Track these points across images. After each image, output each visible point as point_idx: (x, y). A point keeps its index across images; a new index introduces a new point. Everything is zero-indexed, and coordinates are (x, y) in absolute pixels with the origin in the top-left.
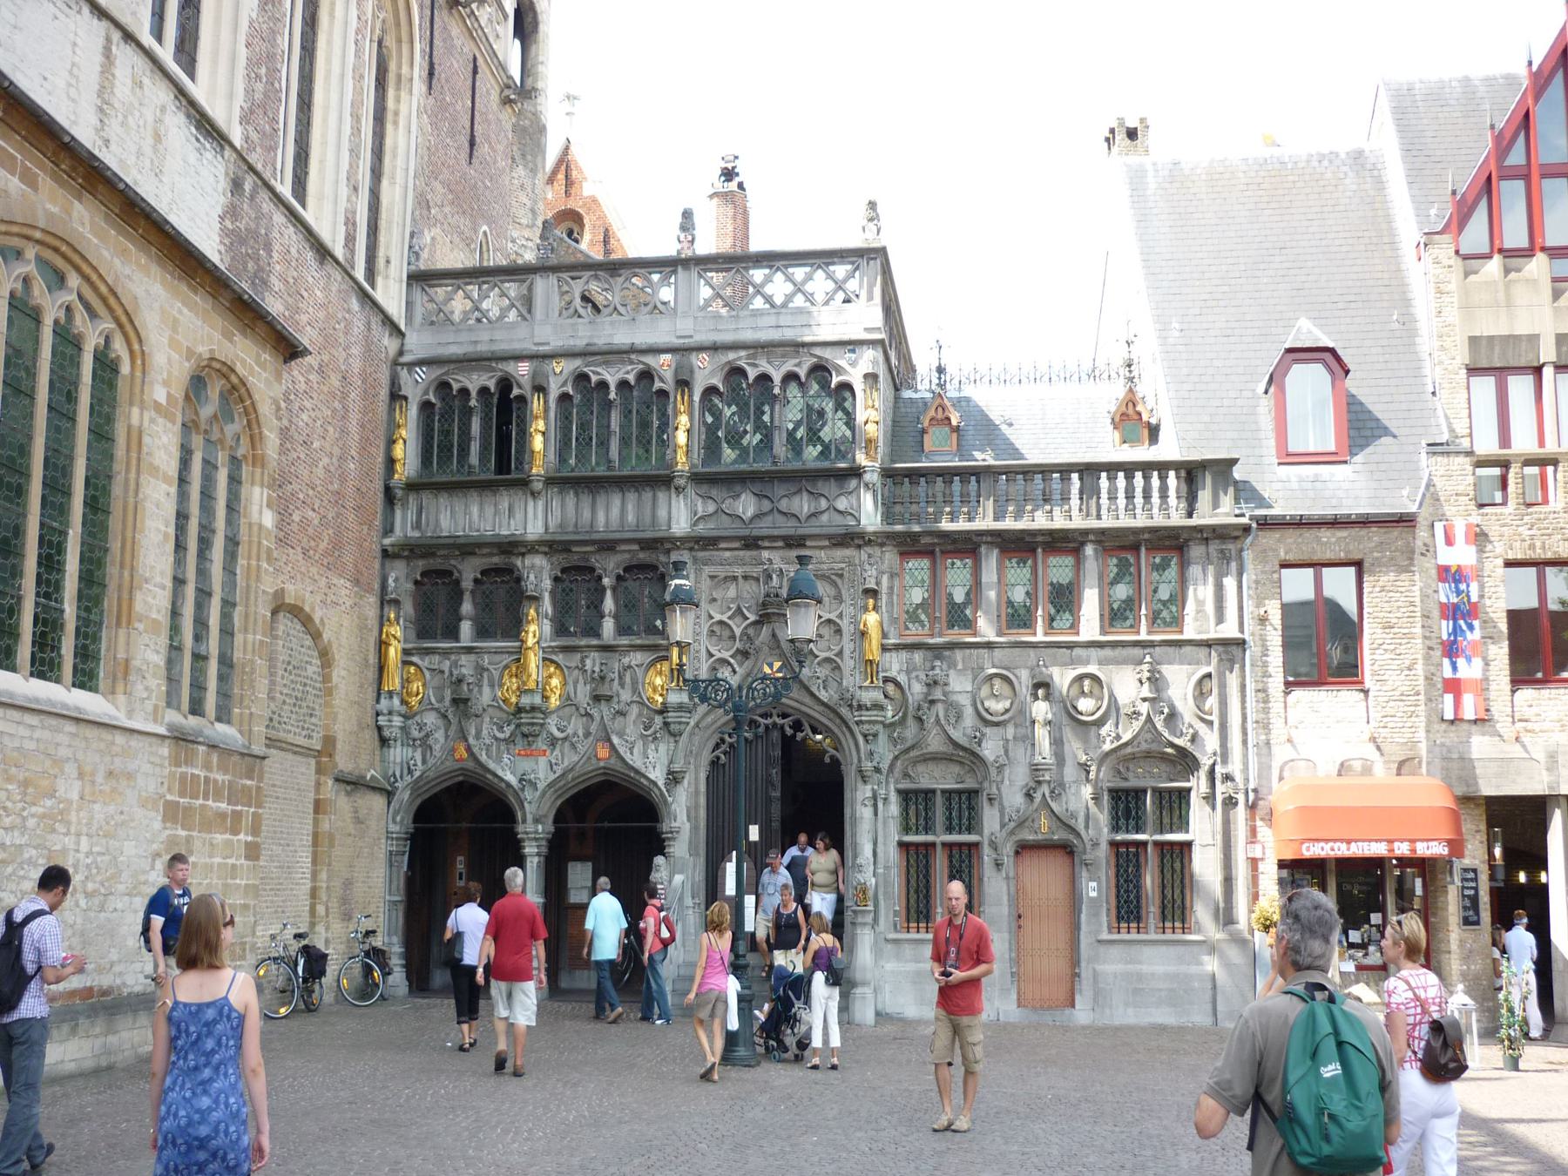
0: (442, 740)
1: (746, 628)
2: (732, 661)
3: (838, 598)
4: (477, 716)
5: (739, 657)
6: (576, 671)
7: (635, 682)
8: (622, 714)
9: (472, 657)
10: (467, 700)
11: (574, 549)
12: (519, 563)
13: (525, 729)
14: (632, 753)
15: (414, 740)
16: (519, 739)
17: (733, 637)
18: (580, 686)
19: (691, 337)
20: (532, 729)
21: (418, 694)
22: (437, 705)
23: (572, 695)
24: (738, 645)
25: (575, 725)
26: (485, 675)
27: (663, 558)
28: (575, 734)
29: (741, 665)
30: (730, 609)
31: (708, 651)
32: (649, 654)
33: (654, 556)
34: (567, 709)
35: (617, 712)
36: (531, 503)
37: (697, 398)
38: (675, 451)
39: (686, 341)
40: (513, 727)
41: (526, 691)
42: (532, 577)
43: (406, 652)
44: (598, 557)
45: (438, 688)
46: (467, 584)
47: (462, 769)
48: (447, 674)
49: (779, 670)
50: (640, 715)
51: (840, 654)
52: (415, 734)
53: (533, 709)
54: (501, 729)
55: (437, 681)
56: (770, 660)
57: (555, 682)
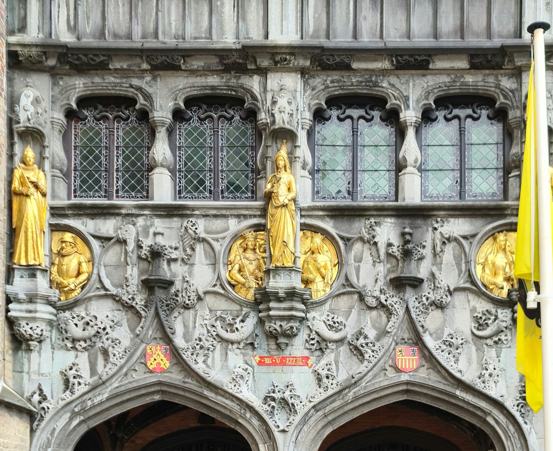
0: (126, 342)
4: (187, 307)
6: (358, 246)
8: (440, 306)
9: (176, 222)
10: (171, 283)
13: (276, 326)
16: (262, 343)
20: (286, 325)
21: (79, 274)
22: (113, 291)
25: (359, 321)
26: (199, 248)
27: (507, 83)
28: (360, 333)
32: (489, 219)
33: (491, 79)
34: (345, 298)
35: (433, 303)
42: (282, 102)
43: (55, 211)
45: (117, 266)
47: (160, 383)
48: (131, 246)
53: (292, 294)
54: (231, 327)
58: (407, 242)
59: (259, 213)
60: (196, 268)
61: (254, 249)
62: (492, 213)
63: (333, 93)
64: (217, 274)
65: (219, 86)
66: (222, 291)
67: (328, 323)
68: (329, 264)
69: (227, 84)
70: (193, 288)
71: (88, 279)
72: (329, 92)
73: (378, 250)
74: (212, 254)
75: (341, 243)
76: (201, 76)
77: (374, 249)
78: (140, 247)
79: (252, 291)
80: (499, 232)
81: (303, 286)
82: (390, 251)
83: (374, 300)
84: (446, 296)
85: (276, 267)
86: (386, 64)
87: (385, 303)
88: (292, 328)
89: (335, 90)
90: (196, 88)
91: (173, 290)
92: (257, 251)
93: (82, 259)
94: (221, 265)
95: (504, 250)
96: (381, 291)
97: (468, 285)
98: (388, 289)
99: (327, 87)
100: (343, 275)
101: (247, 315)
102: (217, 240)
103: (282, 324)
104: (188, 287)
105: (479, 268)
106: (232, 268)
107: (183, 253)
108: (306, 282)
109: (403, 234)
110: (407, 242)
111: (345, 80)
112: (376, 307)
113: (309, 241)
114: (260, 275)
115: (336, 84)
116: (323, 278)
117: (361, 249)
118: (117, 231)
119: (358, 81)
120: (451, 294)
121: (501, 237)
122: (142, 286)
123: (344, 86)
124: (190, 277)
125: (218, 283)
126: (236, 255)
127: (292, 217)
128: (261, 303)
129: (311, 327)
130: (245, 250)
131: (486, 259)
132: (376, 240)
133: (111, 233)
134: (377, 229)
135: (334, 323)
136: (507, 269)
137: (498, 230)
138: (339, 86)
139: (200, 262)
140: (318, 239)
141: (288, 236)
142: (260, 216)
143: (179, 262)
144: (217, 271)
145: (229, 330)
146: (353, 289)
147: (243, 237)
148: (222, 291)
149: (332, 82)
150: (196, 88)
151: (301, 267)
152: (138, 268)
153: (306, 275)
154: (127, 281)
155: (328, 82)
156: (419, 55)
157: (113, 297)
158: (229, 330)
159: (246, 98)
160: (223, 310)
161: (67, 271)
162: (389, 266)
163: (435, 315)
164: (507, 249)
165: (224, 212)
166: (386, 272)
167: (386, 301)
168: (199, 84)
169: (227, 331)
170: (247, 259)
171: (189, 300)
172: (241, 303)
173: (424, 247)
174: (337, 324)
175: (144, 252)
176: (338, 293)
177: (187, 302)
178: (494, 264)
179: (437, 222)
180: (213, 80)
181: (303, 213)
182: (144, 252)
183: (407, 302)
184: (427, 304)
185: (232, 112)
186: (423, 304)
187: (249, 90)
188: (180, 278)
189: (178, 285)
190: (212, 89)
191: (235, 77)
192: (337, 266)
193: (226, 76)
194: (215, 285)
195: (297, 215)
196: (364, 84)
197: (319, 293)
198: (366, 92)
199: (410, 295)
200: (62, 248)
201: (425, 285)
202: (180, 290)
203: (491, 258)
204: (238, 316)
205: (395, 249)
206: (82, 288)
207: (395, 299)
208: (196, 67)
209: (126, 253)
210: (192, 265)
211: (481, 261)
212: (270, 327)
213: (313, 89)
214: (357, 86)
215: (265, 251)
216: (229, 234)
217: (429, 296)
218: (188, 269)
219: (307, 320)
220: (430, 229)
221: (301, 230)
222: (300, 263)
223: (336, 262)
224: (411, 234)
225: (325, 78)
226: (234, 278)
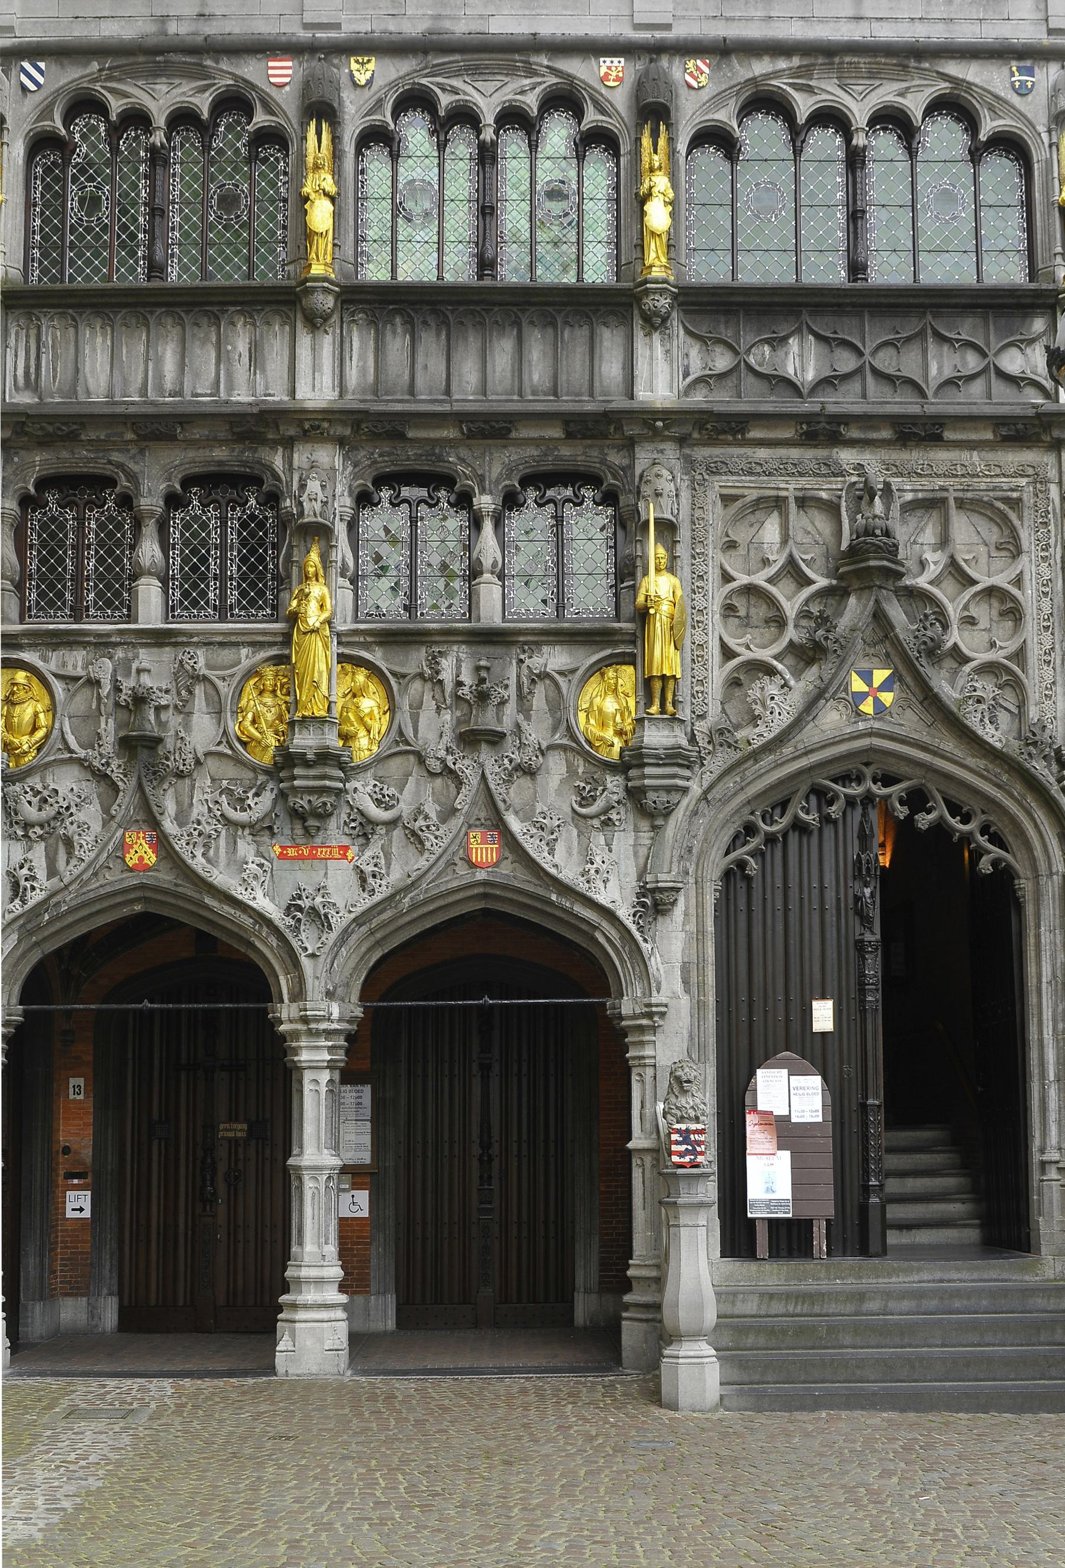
1: (807, 602)
2: (780, 667)
3: (1016, 551)
5: (790, 660)
6: (417, 685)
7: (558, 706)
10: (159, 740)
11: (410, 434)
12: (278, 462)
14: (551, 852)
15: (27, 825)
17: (779, 622)
18: (427, 715)
19: (668, 27)
21: (35, 729)
22: (82, 753)
23: (409, 733)
24: (791, 633)
26: (199, 690)
29: (797, 674)
30: (766, 562)
31: (724, 646)
36: (304, 340)
37: (682, 147)
38: (641, 247)
39: (659, 35)
41: (305, 722)
44: (464, 452)
45: (86, 718)
46: (150, 501)
49: (886, 686)
50: (572, 771)
51: (1020, 655)
52: (31, 813)
53: (325, 757)
55: (82, 701)
56: (864, 665)
57: (371, 703)
58: (482, 681)
60: (195, 718)
61: (274, 692)
62: (598, 639)
64: (222, 726)
66: (230, 752)
68: (376, 711)
70: (189, 748)
71: (47, 736)
73: (443, 691)
74: (216, 698)
75: (393, 681)
77: (437, 689)
78: (117, 689)
79: (271, 751)
80: (607, 666)
81: (341, 743)
82: (460, 693)
83: (438, 763)
84: (537, 757)
86: (450, 433)
87: (452, 766)
88: (325, 804)
91: (160, 747)
92: (279, 692)
93: (40, 708)
94: (229, 714)
95: (615, 691)
96: (447, 750)
97: (565, 741)
98: (458, 747)
100: (395, 727)
102: (224, 679)
104: (183, 746)
105: (582, 716)
106: (244, 718)
107: (176, 699)
108: (346, 737)
109: (478, 669)
110: (482, 681)
112: (441, 773)
113: (348, 678)
114: (282, 727)
116: (369, 731)
117: (420, 689)
118: (87, 667)
120: (543, 755)
121: (610, 673)
122: (120, 746)
124: (186, 731)
125: (224, 740)
126: (249, 700)
127: (326, 646)
128: (283, 768)
130: (261, 693)
131: (591, 703)
132: (440, 677)
133: (80, 672)
134: (444, 661)
136: (618, 719)
137: (607, 663)
139: (200, 710)
140: (361, 677)
141: (320, 673)
143: (171, 710)
146: (409, 748)
148: (230, 752)
151: (337, 716)
152: (115, 720)
153: (346, 728)
154: (100, 738)
156: (497, 422)
157: (80, 762)
161: (20, 725)
162: (458, 713)
163: (523, 782)
164: (620, 689)
166: (454, 722)
167: (454, 764)
170: (265, 705)
171: (184, 765)
172: (254, 769)
173: (506, 687)
175: (123, 697)
176: (389, 752)
177: (181, 768)
178: (600, 710)
179: (524, 652)
181: (344, 639)
182: (123, 697)
183: (482, 765)
184: (510, 768)
186: (505, 769)
188: (172, 733)
189: (170, 743)
194: (220, 743)
195: (332, 642)
199: (486, 755)
200: (13, 693)
201: (509, 739)
202: (172, 750)
203: (597, 701)
205: (466, 690)
206: (39, 749)
207: (466, 762)
209: (99, 698)
210: (190, 714)
211: (584, 706)
215: (288, 694)
217: (513, 756)
218: (183, 719)
220: (514, 662)
222: (336, 710)
224: (488, 669)
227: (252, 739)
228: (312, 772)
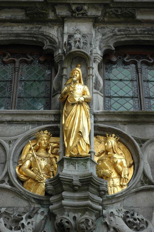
40: (38, 218)
59: (52, 119)
63: (119, 40)
65: (22, 34)
66: (8, 186)
67: (128, 220)
69: (29, 32)
72: (116, 39)
76: (8, 27)
85: (70, 156)
88: (87, 220)
89: (122, 38)
90: (2, 35)
92: (50, 152)
94: (11, 162)
99: (115, 35)
101: (34, 212)
103: (76, 215)
111: (131, 29)
115: (122, 33)
116: (119, 174)
119: (141, 30)
123: (129, 34)
125: (6, 180)
129: (108, 223)
130: (37, 150)
135: (135, 219)
138: (125, 34)
142: (55, 122)
144: (6, 167)
145: (13, 227)
147: (36, 139)
149: (119, 31)
150: (2, 35)
155: (116, 31)
158: (13, 227)
159: (45, 43)
160: (9, 207)
165: (19, 118)
168: (6, 32)
169: (11, 229)
172: (28, 198)
174: (138, 222)
180: (18, 29)
185: (31, 59)
187: (48, 36)
190: (17, 36)
191: (36, 27)
192: (133, 166)
193: (29, 27)
194: (3, 182)
196: (146, 32)
197: (116, 188)
198: (148, 39)
204: (25, 213)
208: (4, 17)
212: (62, 220)
213: (103, 35)
214: (140, 34)
216: (21, 138)
219: (104, 217)
221: (95, 135)
223: (131, 162)
225: (113, 29)
226: (24, 173)
227: (28, 177)
228: (77, 195)
